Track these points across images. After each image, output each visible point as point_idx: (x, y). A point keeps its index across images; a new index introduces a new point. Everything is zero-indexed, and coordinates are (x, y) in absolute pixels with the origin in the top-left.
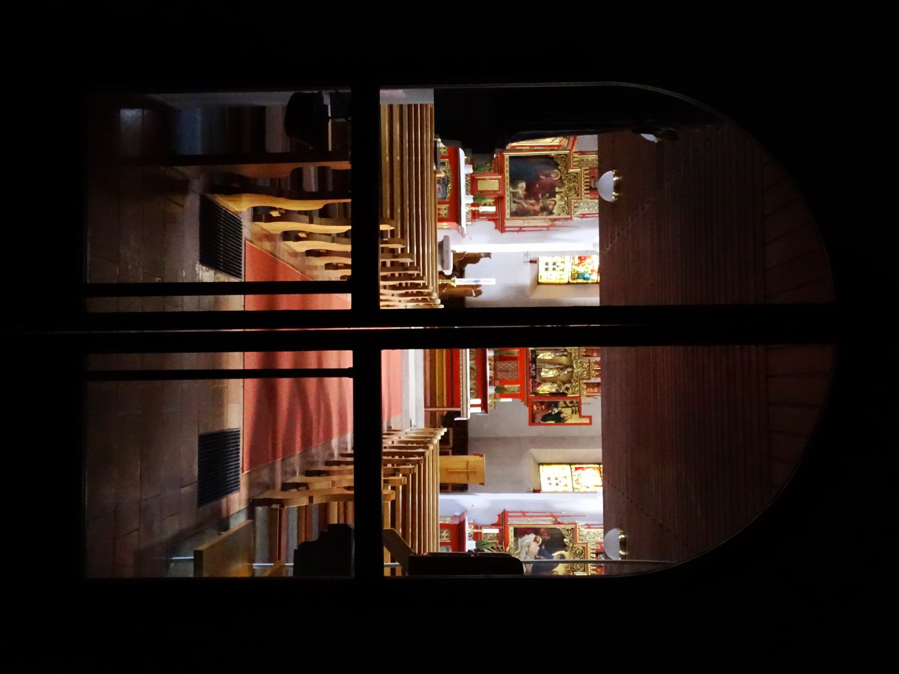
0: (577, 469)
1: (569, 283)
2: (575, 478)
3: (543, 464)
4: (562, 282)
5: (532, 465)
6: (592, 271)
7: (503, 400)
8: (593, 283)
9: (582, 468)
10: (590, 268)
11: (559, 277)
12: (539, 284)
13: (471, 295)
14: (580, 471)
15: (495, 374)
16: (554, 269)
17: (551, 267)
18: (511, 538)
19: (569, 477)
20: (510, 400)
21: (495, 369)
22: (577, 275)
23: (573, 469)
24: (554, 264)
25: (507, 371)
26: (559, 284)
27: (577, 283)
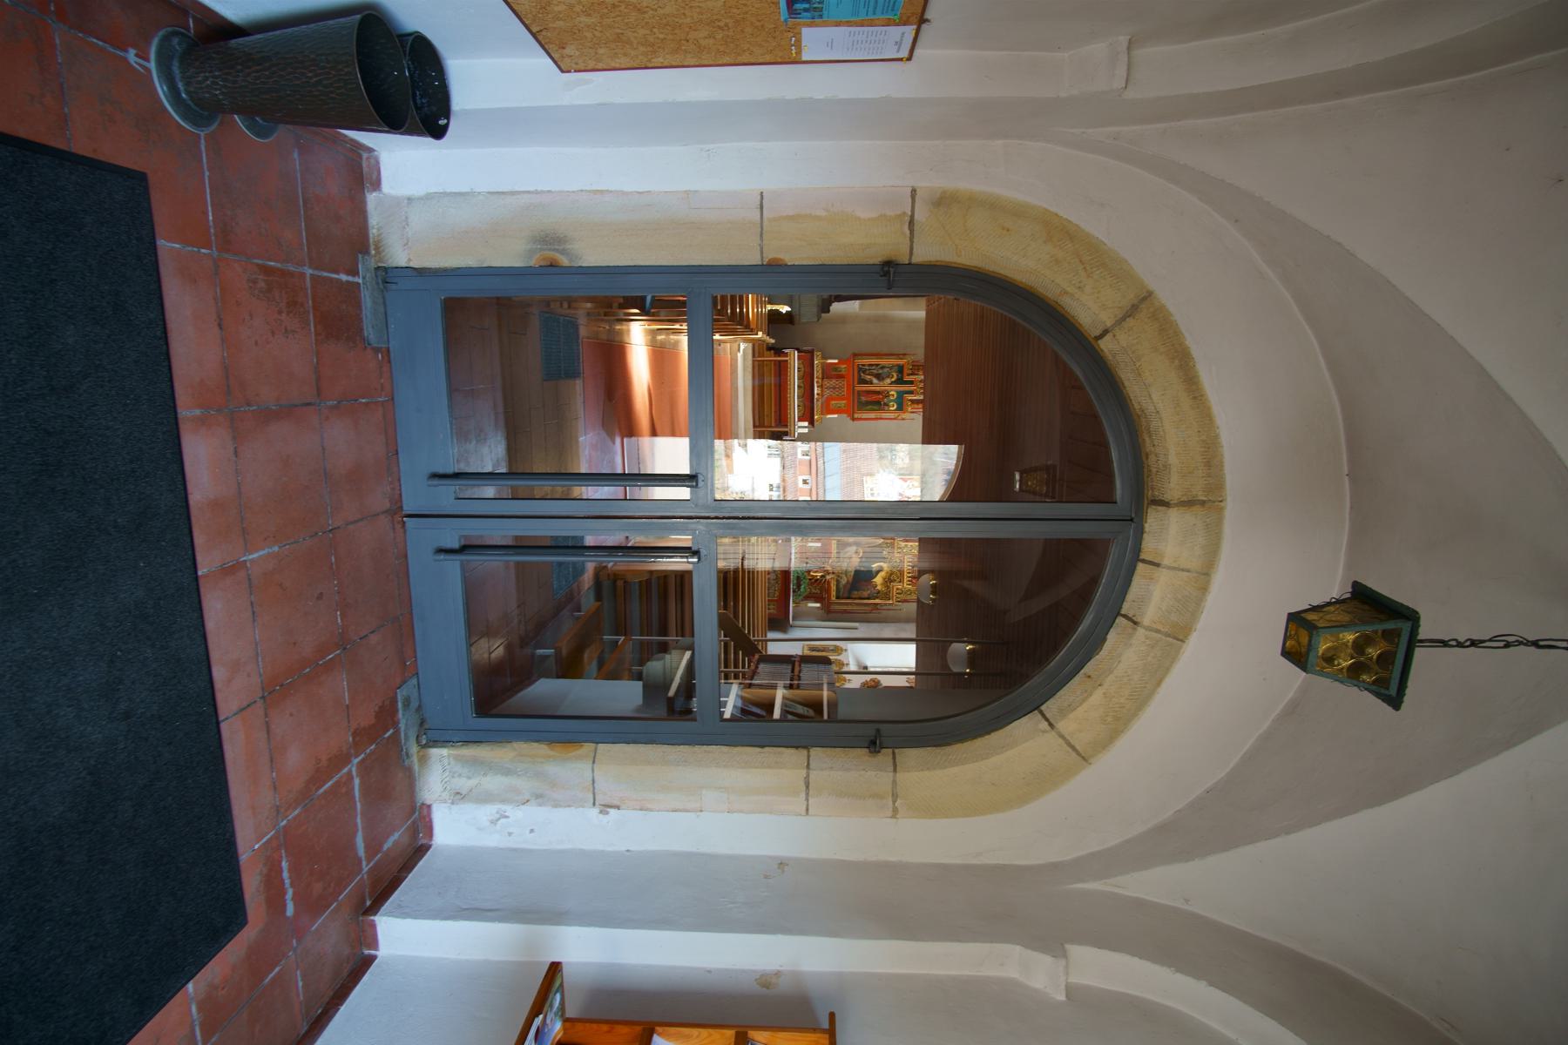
18: (834, 554)
21: (821, 386)
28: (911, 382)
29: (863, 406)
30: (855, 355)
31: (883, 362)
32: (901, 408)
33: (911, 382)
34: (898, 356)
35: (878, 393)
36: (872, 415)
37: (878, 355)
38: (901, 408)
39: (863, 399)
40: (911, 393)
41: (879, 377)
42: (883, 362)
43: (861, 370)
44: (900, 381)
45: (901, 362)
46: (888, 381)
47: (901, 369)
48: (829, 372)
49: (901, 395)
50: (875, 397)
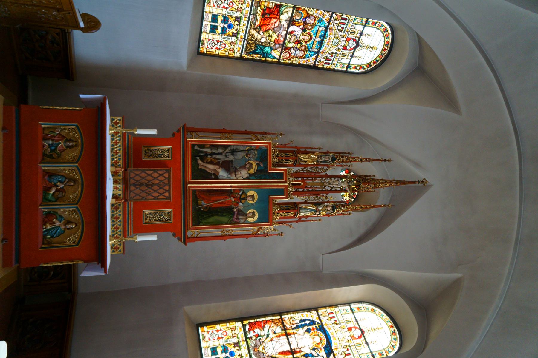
0: (252, 326)
1: (241, 58)
2: (252, 344)
3: (202, 325)
4: (232, 54)
5: (188, 330)
6: (276, 42)
7: (141, 238)
8: (272, 63)
9: (261, 326)
10: (275, 36)
11: (228, 47)
12: (200, 53)
13: (77, 27)
14: (257, 331)
15: (126, 189)
16: (224, 31)
17: (220, 25)
19: (243, 345)
20: (153, 238)
21: (124, 182)
22: (254, 46)
23: (247, 327)
24: (225, 20)
25: (150, 185)
26: (228, 57)
27: (253, 60)
28: (280, 176)
29: (202, 217)
30: (186, 130)
31: (235, 142)
32: (265, 218)
33: (280, 176)
34: (254, 134)
35: (228, 193)
36: (217, 231)
37: (222, 132)
38: (265, 218)
39: (203, 204)
40: (280, 192)
41: (228, 166)
42: (235, 142)
43: (199, 154)
44: (262, 174)
45: (263, 143)
46: (244, 173)
47: (263, 156)
48: (136, 155)
49: (265, 197)
50: (221, 201)
